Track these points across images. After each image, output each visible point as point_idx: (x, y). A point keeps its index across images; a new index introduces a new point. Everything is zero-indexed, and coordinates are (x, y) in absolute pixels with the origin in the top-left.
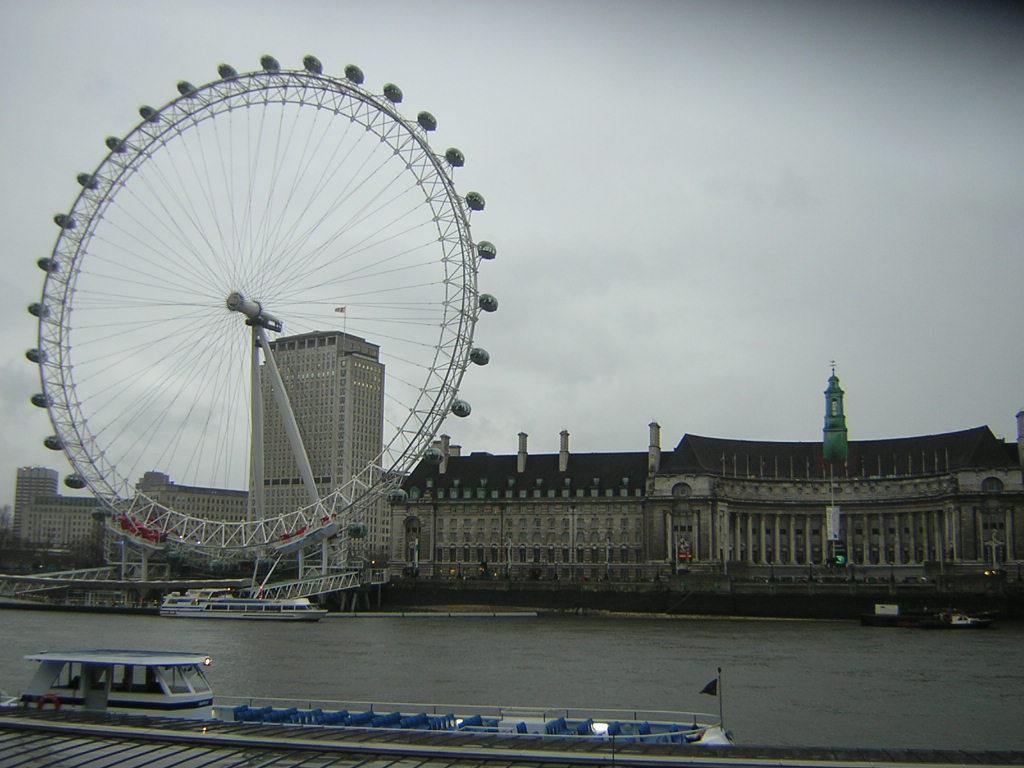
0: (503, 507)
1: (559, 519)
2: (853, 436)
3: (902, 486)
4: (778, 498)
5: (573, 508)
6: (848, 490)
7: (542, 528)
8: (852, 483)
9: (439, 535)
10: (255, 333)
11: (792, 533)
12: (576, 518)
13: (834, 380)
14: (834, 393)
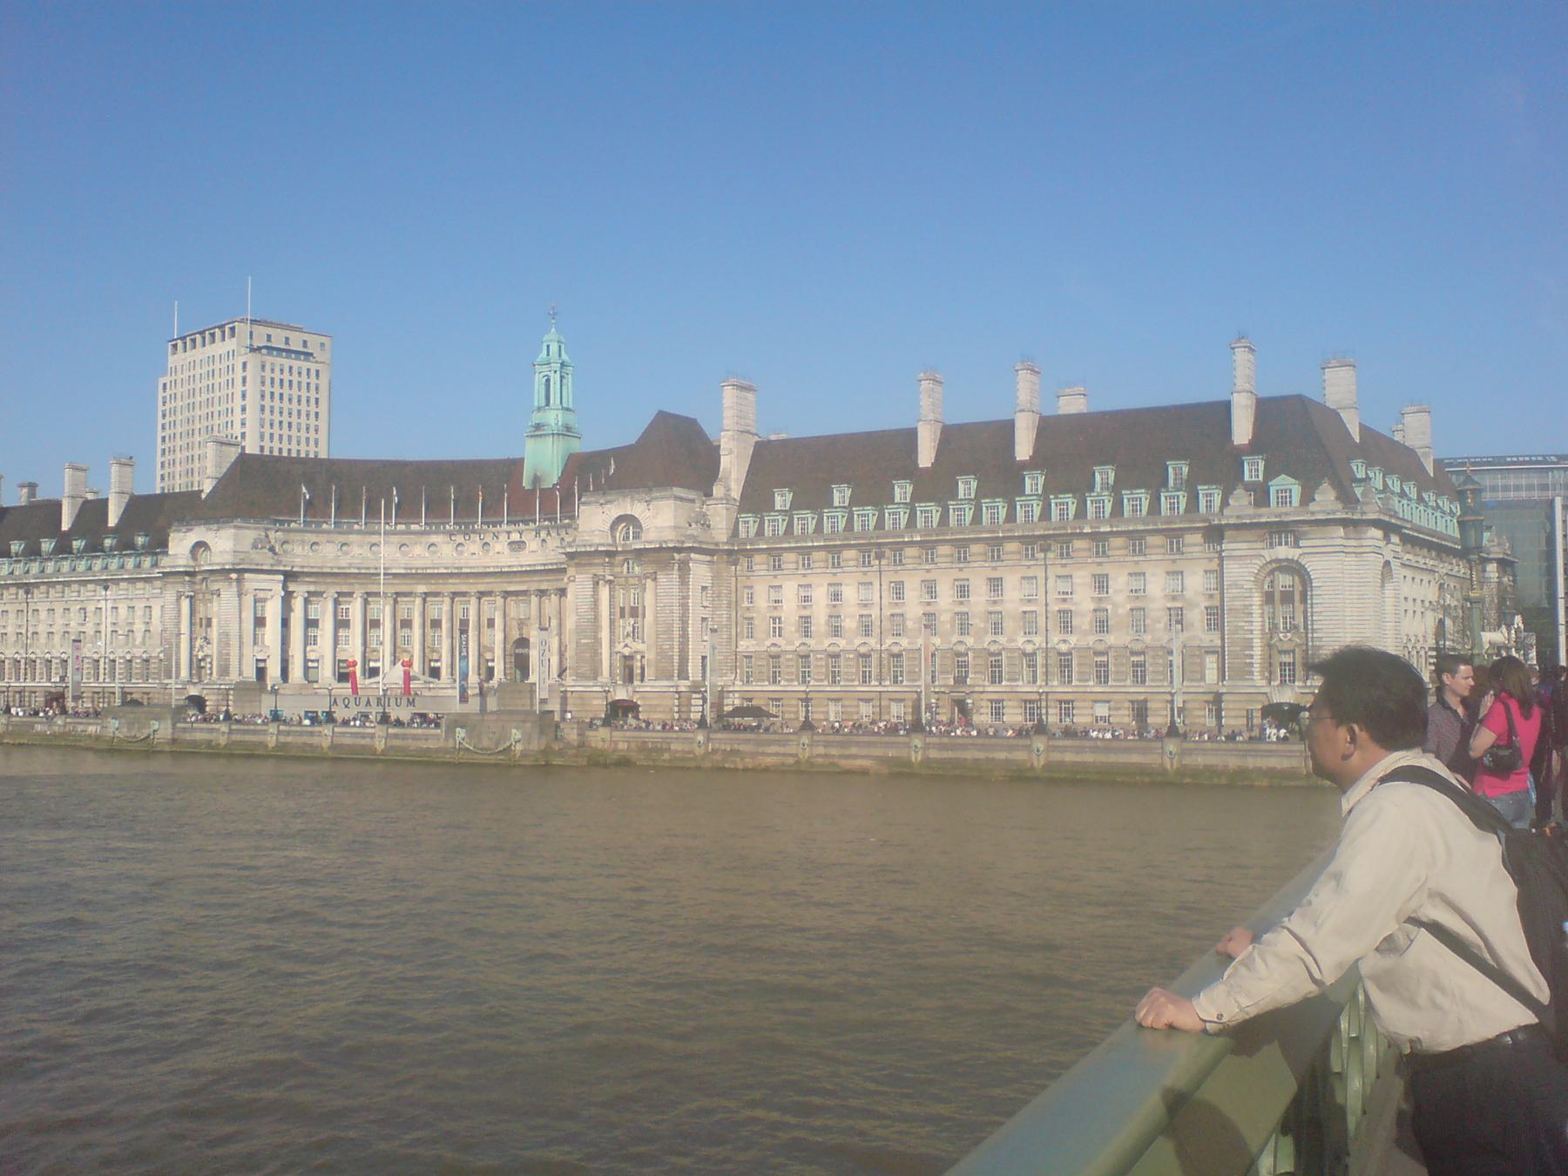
0: (28, 588)
1: (91, 608)
4: (419, 563)
5: (106, 588)
6: (533, 544)
7: (73, 624)
8: (538, 533)
11: (445, 625)
12: (110, 604)
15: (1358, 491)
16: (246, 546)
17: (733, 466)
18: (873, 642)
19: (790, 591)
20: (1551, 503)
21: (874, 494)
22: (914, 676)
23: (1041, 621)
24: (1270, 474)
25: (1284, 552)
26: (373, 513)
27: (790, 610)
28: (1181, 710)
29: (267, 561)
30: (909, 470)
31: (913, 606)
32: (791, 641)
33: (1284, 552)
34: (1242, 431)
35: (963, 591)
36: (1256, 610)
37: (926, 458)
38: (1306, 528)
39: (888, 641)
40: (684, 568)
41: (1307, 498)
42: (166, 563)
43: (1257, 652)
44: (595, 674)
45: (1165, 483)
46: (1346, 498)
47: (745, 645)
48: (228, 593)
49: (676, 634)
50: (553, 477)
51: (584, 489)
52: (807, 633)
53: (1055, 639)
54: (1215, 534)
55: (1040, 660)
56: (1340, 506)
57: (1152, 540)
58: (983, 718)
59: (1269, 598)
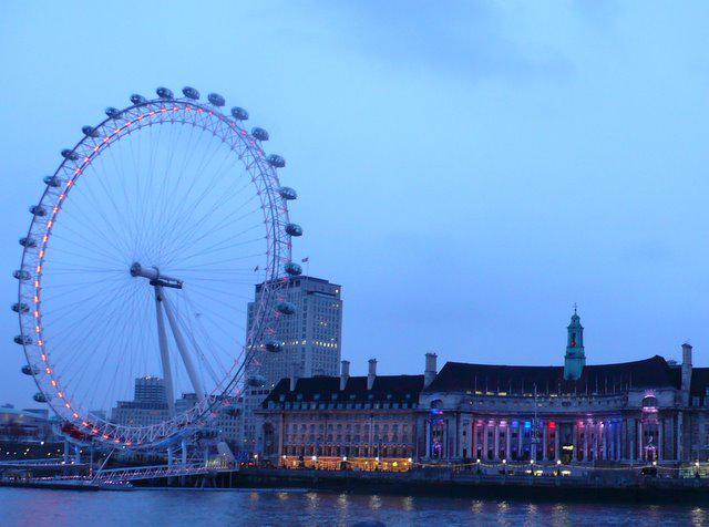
0: (327, 416)
1: (363, 425)
2: (590, 361)
3: (608, 402)
9: (285, 436)
10: (157, 291)
13: (575, 318)
14: (575, 331)
16: (458, 401)
17: (686, 377)
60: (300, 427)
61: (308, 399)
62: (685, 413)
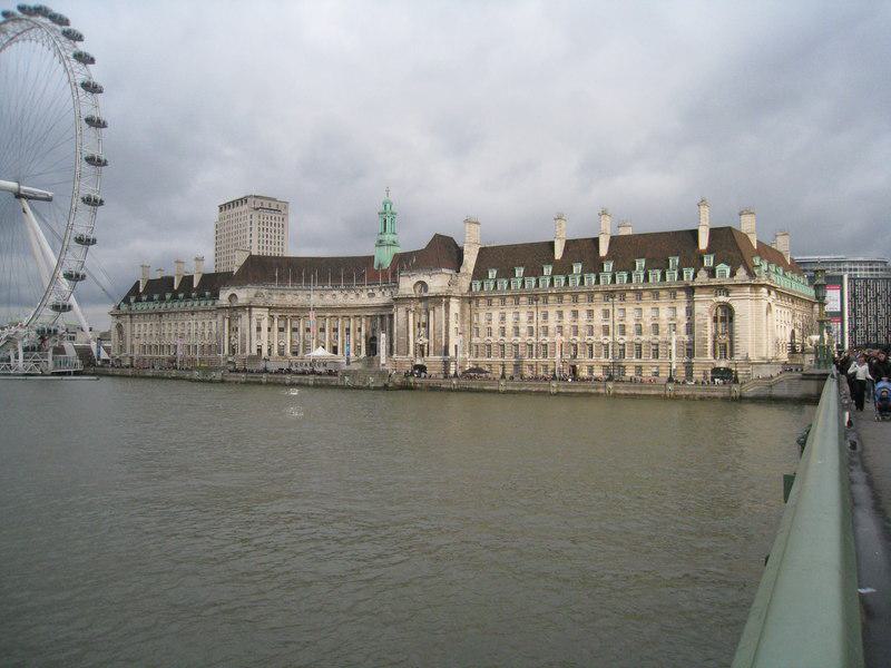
0: (160, 314)
1: (186, 323)
6: (379, 294)
15: (756, 271)
17: (470, 260)
18: (533, 339)
19: (496, 315)
20: (842, 277)
21: (534, 271)
22: (554, 354)
23: (611, 330)
24: (716, 263)
25: (722, 299)
26: (308, 281)
27: (496, 324)
28: (675, 370)
29: (260, 301)
30: (550, 259)
31: (552, 322)
32: (496, 338)
33: (722, 299)
34: (703, 243)
35: (575, 314)
36: (709, 325)
37: (558, 254)
38: (731, 288)
39: (541, 338)
40: (447, 306)
41: (733, 274)
42: (218, 303)
43: (710, 344)
44: (408, 352)
45: (668, 267)
46: (751, 274)
47: (475, 340)
48: (245, 317)
49: (443, 332)
50: (387, 263)
51: (402, 269)
52: (503, 335)
53: (618, 337)
54: (690, 290)
55: (610, 348)
56: (747, 278)
57: (662, 293)
58: (584, 373)
59: (715, 320)
60: (142, 327)
61: (150, 299)
62: (462, 298)
